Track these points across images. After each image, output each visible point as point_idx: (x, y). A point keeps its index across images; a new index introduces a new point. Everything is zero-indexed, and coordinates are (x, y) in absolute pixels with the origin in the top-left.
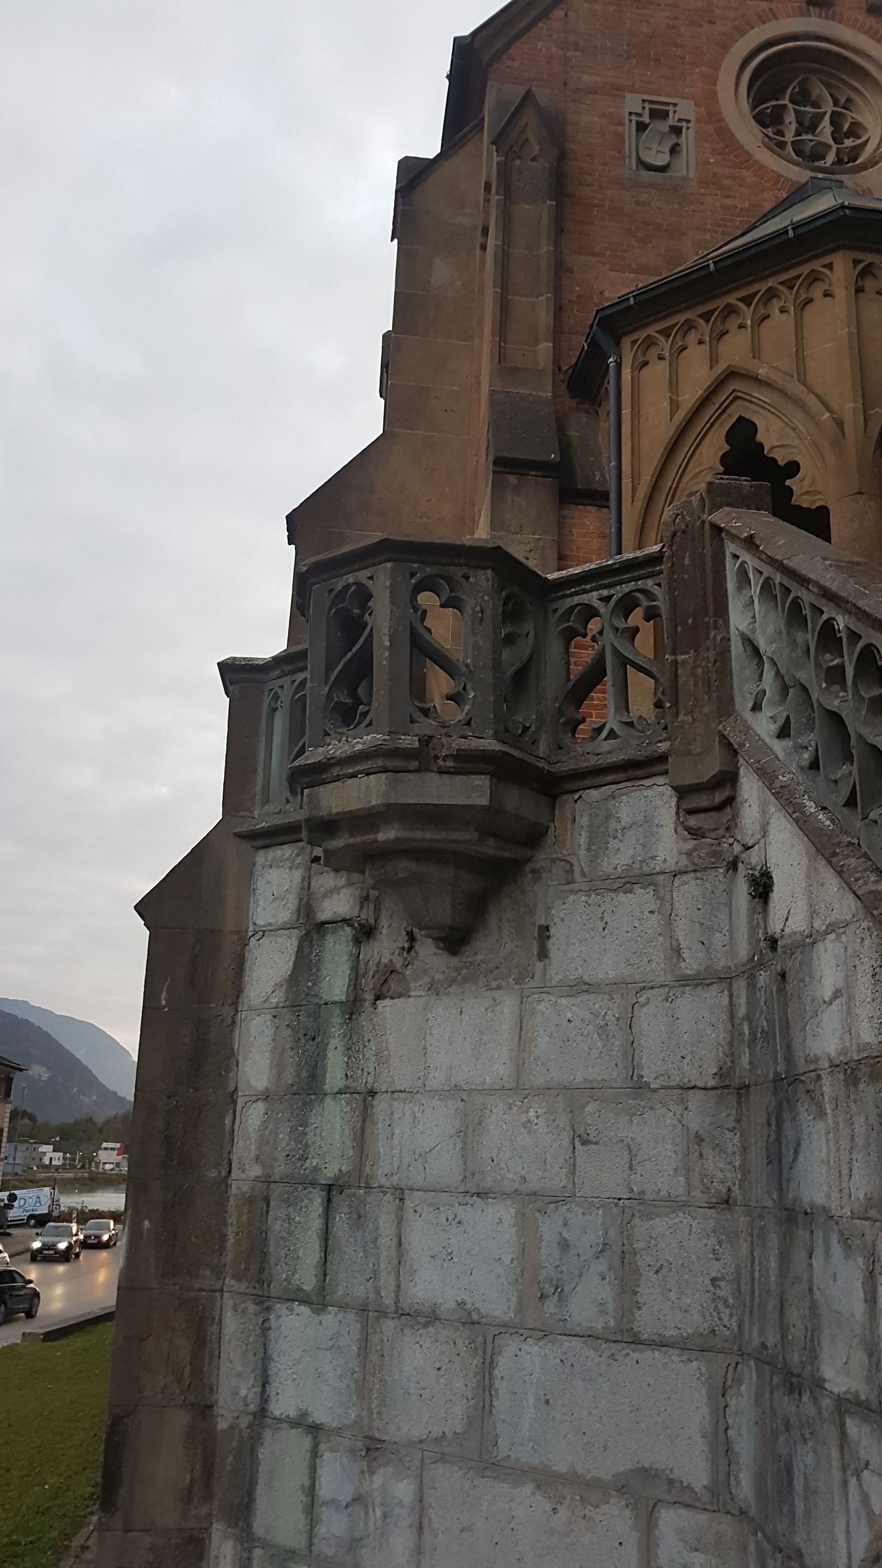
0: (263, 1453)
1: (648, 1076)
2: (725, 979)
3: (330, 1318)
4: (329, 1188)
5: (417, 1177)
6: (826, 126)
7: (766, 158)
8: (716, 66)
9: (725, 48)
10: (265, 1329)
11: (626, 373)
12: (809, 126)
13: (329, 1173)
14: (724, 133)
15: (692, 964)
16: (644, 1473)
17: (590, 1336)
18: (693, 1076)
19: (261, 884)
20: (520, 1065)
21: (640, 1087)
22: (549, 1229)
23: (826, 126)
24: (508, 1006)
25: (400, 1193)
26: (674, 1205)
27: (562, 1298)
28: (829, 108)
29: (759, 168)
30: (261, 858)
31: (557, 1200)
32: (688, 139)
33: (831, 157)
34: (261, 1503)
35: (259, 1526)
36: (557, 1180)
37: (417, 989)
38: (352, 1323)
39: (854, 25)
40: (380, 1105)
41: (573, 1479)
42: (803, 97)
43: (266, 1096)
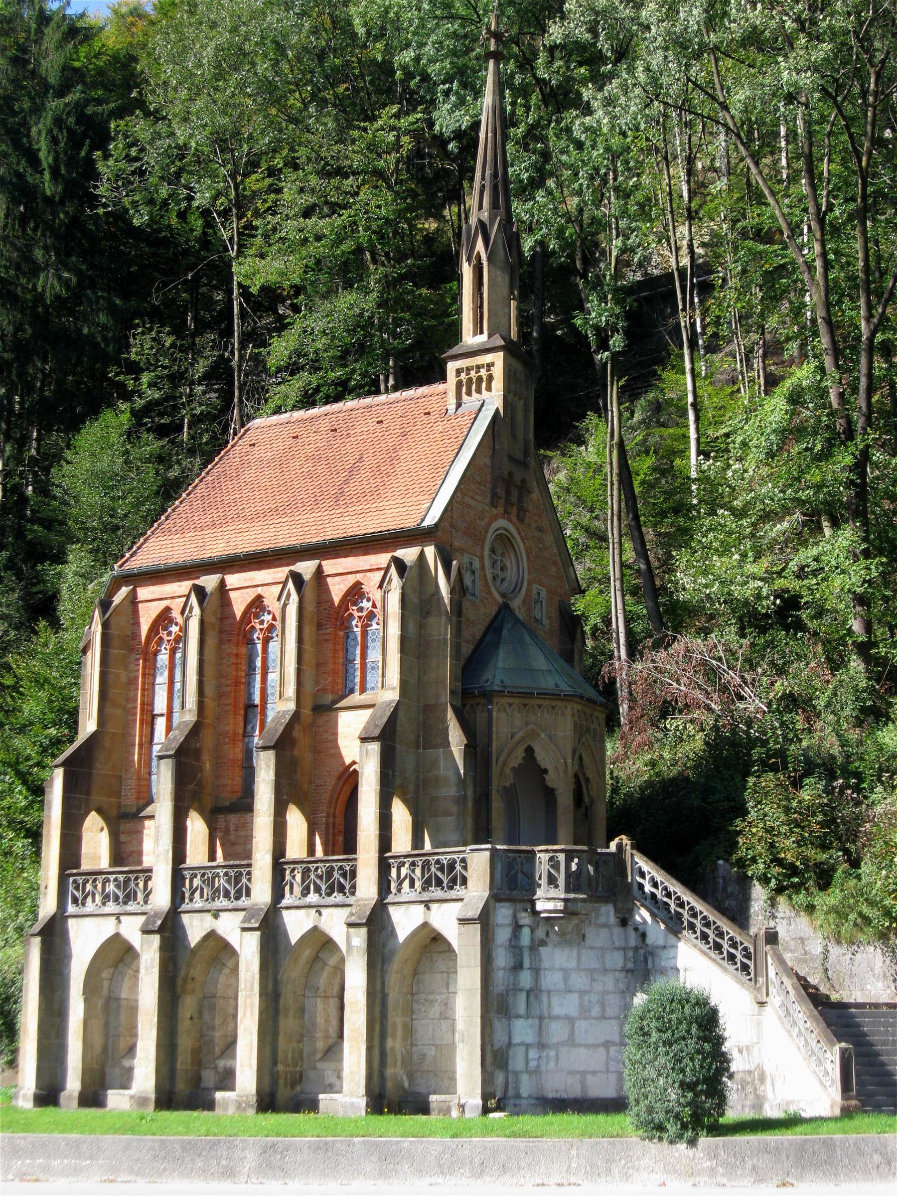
0: (511, 1053)
2: (624, 949)
3: (530, 1021)
4: (528, 992)
5: (553, 988)
8: (484, 541)
9: (486, 532)
10: (509, 1025)
11: (494, 713)
13: (528, 987)
14: (485, 575)
15: (617, 944)
16: (608, 1042)
17: (595, 1019)
19: (498, 912)
20: (578, 965)
21: (606, 970)
22: (586, 998)
24: (575, 951)
25: (549, 992)
27: (589, 1011)
29: (490, 593)
30: (497, 904)
31: (588, 992)
34: (510, 1062)
35: (510, 1068)
36: (588, 988)
37: (550, 945)
38: (537, 1021)
39: (514, 524)
40: (542, 972)
41: (593, 1045)
43: (504, 969)
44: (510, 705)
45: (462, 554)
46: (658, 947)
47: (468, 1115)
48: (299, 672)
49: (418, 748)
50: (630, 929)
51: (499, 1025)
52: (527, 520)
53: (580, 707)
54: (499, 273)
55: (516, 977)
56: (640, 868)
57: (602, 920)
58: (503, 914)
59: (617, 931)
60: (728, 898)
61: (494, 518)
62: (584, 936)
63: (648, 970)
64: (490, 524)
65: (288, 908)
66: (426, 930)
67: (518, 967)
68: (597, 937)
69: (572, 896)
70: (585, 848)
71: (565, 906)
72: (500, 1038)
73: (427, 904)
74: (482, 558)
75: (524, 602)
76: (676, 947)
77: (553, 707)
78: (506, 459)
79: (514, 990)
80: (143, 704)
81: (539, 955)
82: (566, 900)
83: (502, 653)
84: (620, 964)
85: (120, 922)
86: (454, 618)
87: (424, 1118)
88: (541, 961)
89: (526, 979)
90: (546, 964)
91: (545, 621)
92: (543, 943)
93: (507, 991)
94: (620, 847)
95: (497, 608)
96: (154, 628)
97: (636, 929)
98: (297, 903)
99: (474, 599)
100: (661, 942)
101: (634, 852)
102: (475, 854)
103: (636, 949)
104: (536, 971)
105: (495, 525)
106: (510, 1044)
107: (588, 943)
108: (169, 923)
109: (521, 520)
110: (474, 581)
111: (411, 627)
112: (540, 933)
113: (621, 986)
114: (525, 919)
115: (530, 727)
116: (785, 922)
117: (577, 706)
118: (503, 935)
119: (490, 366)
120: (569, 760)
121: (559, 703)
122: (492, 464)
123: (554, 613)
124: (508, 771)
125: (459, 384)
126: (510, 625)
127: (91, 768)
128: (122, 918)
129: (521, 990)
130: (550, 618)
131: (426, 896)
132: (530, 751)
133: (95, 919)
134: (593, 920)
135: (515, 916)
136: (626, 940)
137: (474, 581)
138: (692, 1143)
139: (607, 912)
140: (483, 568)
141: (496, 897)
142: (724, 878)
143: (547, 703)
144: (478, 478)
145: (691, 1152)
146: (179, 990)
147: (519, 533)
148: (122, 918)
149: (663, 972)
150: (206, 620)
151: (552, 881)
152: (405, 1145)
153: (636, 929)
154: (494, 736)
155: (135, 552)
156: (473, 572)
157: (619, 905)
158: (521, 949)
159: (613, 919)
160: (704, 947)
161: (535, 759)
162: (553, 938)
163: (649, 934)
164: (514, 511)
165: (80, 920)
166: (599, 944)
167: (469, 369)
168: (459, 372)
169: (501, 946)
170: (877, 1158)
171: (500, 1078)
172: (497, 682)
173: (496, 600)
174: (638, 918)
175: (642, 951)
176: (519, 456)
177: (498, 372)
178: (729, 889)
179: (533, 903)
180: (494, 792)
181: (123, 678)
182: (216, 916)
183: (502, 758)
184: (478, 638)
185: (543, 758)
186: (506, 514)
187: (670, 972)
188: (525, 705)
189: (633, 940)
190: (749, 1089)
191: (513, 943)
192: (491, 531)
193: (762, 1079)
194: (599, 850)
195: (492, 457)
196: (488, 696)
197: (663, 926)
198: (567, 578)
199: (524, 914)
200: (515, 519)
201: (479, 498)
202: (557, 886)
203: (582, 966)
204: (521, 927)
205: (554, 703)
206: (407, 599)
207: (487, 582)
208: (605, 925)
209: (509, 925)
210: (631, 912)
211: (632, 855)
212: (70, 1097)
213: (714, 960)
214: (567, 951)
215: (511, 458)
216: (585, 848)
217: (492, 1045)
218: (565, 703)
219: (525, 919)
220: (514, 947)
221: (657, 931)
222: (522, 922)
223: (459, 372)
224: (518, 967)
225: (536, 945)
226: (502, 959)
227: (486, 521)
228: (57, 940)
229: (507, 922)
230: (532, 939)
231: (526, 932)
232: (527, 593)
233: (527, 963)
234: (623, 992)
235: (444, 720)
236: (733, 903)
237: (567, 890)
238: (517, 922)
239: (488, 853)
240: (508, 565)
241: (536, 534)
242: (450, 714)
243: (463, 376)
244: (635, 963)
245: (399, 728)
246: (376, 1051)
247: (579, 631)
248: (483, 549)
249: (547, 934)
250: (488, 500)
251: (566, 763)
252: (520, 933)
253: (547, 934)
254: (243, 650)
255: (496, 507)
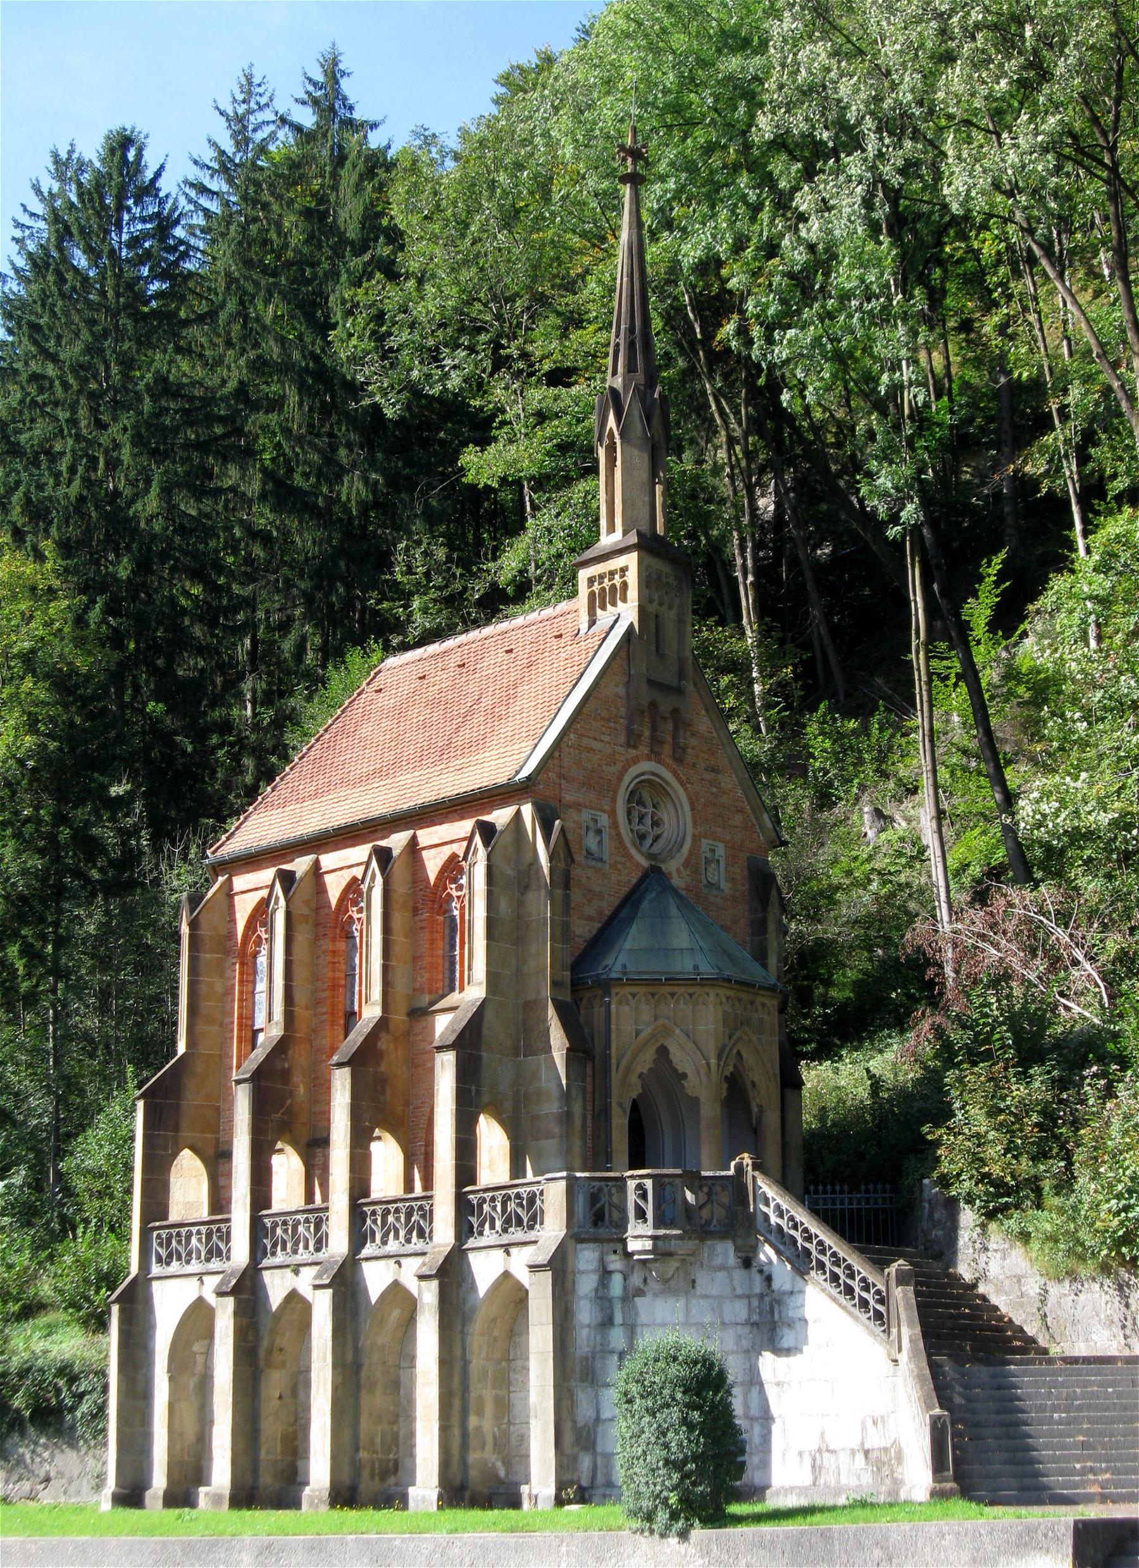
0: (599, 1430)
1: (726, 1319)
2: (748, 1297)
6: (648, 821)
7: (633, 852)
8: (615, 792)
9: (620, 780)
10: (596, 1396)
11: (613, 1007)
12: (642, 818)
14: (618, 834)
15: (739, 1291)
18: (738, 1320)
21: (723, 1324)
23: (648, 821)
26: (733, 1352)
28: (650, 810)
29: (630, 857)
30: (579, 1246)
32: (605, 835)
33: (649, 841)
35: (599, 1449)
39: (667, 767)
40: (639, 1329)
42: (641, 803)
43: (589, 1326)
44: (634, 995)
45: (579, 811)
46: (784, 1293)
47: (540, 1506)
48: (386, 969)
49: (517, 1055)
50: (754, 1270)
51: (583, 1397)
52: (689, 759)
53: (730, 993)
54: (636, 452)
55: (604, 1336)
56: (764, 1193)
57: (719, 1260)
58: (587, 1258)
59: (739, 1274)
60: (934, 1227)
61: (635, 760)
62: (694, 1282)
63: (775, 1323)
64: (624, 770)
65: (367, 1259)
66: (508, 1284)
67: (607, 1322)
68: (711, 1283)
69: (661, 1232)
70: (678, 1171)
71: (655, 1245)
72: (584, 1412)
73: (506, 1248)
74: (613, 813)
75: (687, 863)
76: (802, 1292)
77: (691, 995)
78: (644, 686)
79: (602, 1351)
80: (240, 1017)
81: (635, 1307)
82: (654, 1238)
83: (634, 930)
84: (743, 1315)
85: (202, 1283)
86: (559, 892)
87: (511, 1513)
88: (637, 1314)
89: (617, 1338)
90: (643, 1318)
91: (724, 885)
92: (640, 1293)
93: (594, 1353)
94: (740, 1168)
95: (640, 874)
96: (251, 925)
97: (761, 1271)
98: (378, 1253)
99: (600, 865)
100: (787, 1287)
101: (757, 1173)
102: (552, 1184)
103: (761, 1296)
104: (631, 1329)
105: (634, 771)
106: (598, 1419)
107: (699, 1290)
108: (248, 1283)
109: (680, 761)
110: (600, 842)
111: (504, 906)
112: (636, 1280)
113: (745, 1343)
114: (615, 1263)
115: (660, 1022)
116: (998, 1255)
117: (722, 992)
118: (586, 1285)
119: (624, 570)
120: (713, 1061)
121: (698, 990)
122: (628, 693)
123: (740, 872)
124: (634, 1078)
125: (592, 596)
126: (654, 894)
127: (179, 1098)
128: (205, 1278)
129: (612, 1352)
130: (733, 880)
131: (506, 1239)
132: (663, 1051)
133: (183, 1280)
134: (706, 1261)
135: (602, 1261)
136: (751, 1286)
137: (600, 842)
138: (684, 1535)
139: (725, 1252)
140: (615, 825)
141: (575, 1236)
142: (930, 1201)
143: (682, 990)
144: (604, 714)
145: (683, 1548)
146: (262, 1364)
147: (677, 776)
148: (205, 1278)
149: (790, 1325)
150: (295, 911)
151: (641, 1214)
152: (397, 1543)
153: (761, 1271)
154: (613, 1035)
155: (233, 834)
156: (599, 832)
157: (740, 1242)
158: (610, 1300)
159: (732, 1260)
160: (834, 1292)
161: (670, 1062)
162: (652, 1284)
163: (774, 1276)
164: (667, 749)
165: (163, 1282)
166: (714, 1292)
167: (601, 577)
168: (591, 581)
169: (585, 1297)
170: (877, 1553)
171: (585, 1462)
172: (618, 967)
173: (638, 865)
174: (762, 1257)
175: (767, 1299)
176: (670, 678)
177: (632, 578)
178: (936, 1216)
179: (624, 1242)
180: (614, 1106)
181: (219, 988)
182: (296, 1272)
183: (624, 1063)
184: (608, 913)
185: (682, 1058)
186: (655, 755)
187: (798, 1325)
188: (653, 995)
189: (758, 1285)
190: (886, 1471)
191: (600, 1294)
192: (627, 779)
193: (899, 1457)
194: (704, 1173)
195: (627, 685)
196: (606, 986)
197: (789, 1267)
198: (761, 827)
199: (613, 1257)
200: (670, 761)
201: (606, 738)
202: (646, 1221)
203: (692, 1321)
204: (610, 1273)
205: (691, 990)
206: (496, 871)
207: (622, 843)
208: (723, 1268)
209: (594, 1271)
210: (755, 1249)
211: (754, 1178)
212: (155, 1497)
213: (844, 1308)
214: (671, 1301)
215: (652, 683)
216: (678, 1171)
217: (574, 1422)
218: (706, 989)
219: (615, 1263)
220: (601, 1298)
221: (783, 1272)
222: (611, 1267)
223: (591, 581)
224: (607, 1322)
225: (629, 1296)
226: (585, 1314)
227: (619, 766)
228: (140, 1307)
229: (591, 1268)
230: (625, 1287)
231: (617, 1281)
232: (691, 853)
233: (618, 1318)
234: (747, 1351)
235: (544, 1020)
236: (940, 1233)
237: (656, 1226)
238: (604, 1268)
239: (563, 1183)
240: (665, 818)
241: (707, 776)
242: (551, 1012)
243: (596, 587)
244: (760, 1313)
245: (485, 1032)
246: (456, 1431)
247: (774, 892)
248: (614, 801)
249: (645, 1280)
250: (622, 739)
251: (708, 1065)
252: (609, 1281)
253: (645, 1280)
254: (342, 945)
255: (635, 747)
